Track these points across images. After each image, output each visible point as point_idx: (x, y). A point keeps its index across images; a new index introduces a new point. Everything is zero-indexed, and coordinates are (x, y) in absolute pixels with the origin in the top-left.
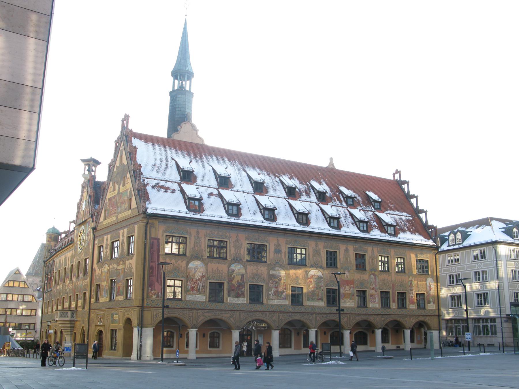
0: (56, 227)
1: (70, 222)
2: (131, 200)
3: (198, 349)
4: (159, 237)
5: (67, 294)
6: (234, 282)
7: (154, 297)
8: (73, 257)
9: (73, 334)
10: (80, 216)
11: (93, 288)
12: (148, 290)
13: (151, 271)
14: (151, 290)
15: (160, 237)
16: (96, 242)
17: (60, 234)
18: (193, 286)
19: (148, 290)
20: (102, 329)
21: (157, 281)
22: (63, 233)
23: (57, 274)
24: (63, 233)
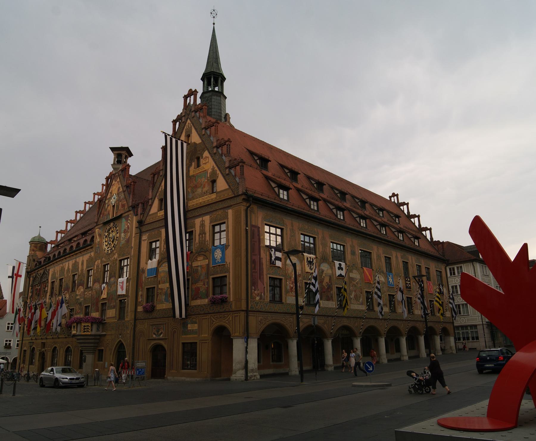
0: (41, 235)
1: (57, 232)
2: (214, 182)
3: (262, 364)
4: (259, 226)
5: (80, 304)
6: (324, 284)
7: (258, 298)
8: (91, 261)
9: (97, 353)
10: (106, 213)
11: (140, 293)
12: (251, 289)
13: (253, 265)
14: (255, 290)
15: (260, 225)
16: (144, 237)
17: (46, 244)
18: (292, 286)
19: (251, 289)
20: (162, 342)
21: (260, 279)
22: (49, 243)
23: (57, 284)
24: (49, 243)
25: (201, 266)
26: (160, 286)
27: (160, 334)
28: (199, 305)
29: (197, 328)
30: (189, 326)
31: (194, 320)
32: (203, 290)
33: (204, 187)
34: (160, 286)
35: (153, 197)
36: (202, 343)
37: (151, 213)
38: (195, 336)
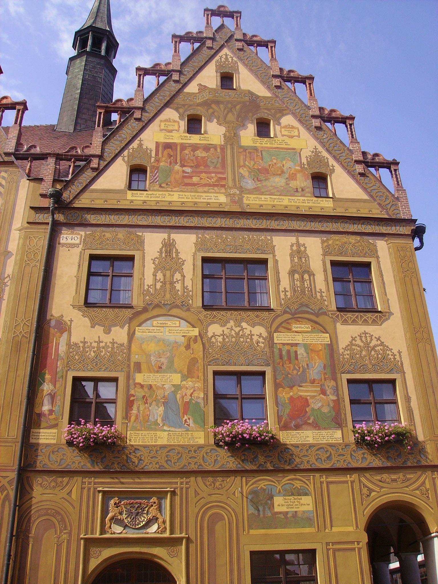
11: (47, 387)
16: (67, 237)
25: (306, 346)
26: (139, 378)
27: (148, 524)
28: (311, 446)
29: (310, 508)
30: (278, 500)
31: (298, 484)
32: (319, 403)
33: (293, 177)
34: (139, 378)
35: (108, 157)
36: (335, 551)
37: (94, 187)
38: (307, 530)
